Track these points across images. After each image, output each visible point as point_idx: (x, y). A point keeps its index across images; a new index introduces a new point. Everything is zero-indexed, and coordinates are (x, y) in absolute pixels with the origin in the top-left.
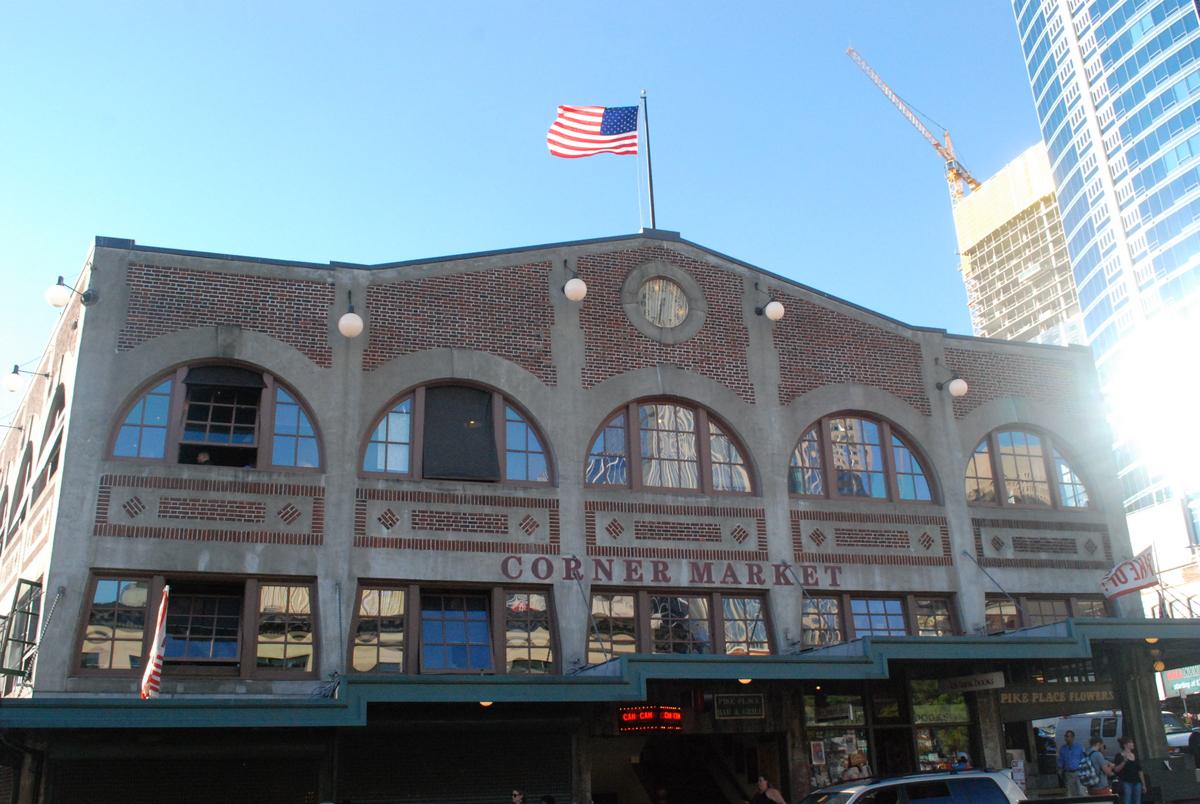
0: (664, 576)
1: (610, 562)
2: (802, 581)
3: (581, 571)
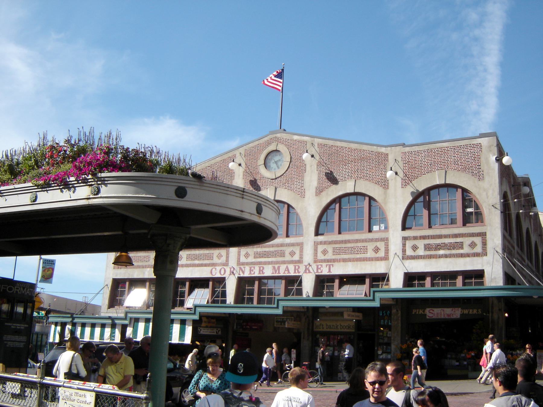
0: (298, 271)
1: (244, 267)
2: (315, 271)
3: (235, 272)
